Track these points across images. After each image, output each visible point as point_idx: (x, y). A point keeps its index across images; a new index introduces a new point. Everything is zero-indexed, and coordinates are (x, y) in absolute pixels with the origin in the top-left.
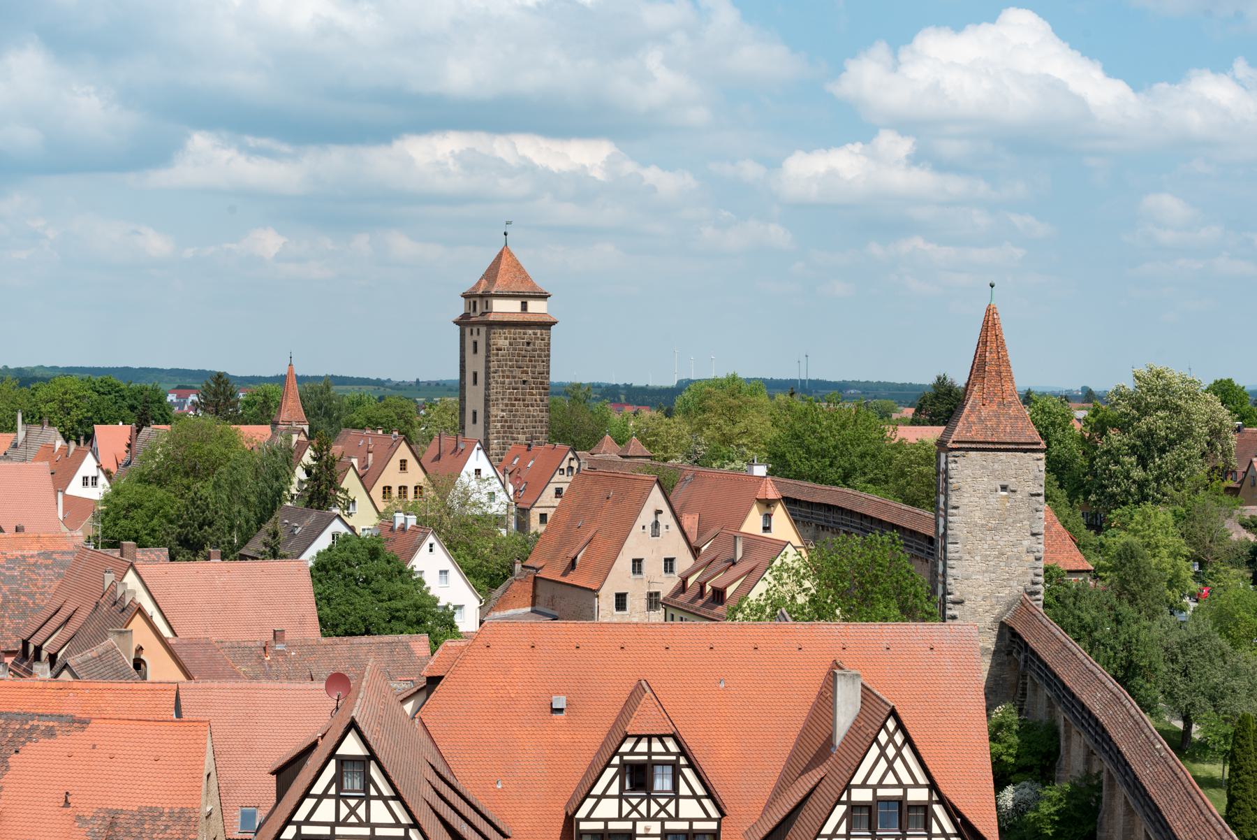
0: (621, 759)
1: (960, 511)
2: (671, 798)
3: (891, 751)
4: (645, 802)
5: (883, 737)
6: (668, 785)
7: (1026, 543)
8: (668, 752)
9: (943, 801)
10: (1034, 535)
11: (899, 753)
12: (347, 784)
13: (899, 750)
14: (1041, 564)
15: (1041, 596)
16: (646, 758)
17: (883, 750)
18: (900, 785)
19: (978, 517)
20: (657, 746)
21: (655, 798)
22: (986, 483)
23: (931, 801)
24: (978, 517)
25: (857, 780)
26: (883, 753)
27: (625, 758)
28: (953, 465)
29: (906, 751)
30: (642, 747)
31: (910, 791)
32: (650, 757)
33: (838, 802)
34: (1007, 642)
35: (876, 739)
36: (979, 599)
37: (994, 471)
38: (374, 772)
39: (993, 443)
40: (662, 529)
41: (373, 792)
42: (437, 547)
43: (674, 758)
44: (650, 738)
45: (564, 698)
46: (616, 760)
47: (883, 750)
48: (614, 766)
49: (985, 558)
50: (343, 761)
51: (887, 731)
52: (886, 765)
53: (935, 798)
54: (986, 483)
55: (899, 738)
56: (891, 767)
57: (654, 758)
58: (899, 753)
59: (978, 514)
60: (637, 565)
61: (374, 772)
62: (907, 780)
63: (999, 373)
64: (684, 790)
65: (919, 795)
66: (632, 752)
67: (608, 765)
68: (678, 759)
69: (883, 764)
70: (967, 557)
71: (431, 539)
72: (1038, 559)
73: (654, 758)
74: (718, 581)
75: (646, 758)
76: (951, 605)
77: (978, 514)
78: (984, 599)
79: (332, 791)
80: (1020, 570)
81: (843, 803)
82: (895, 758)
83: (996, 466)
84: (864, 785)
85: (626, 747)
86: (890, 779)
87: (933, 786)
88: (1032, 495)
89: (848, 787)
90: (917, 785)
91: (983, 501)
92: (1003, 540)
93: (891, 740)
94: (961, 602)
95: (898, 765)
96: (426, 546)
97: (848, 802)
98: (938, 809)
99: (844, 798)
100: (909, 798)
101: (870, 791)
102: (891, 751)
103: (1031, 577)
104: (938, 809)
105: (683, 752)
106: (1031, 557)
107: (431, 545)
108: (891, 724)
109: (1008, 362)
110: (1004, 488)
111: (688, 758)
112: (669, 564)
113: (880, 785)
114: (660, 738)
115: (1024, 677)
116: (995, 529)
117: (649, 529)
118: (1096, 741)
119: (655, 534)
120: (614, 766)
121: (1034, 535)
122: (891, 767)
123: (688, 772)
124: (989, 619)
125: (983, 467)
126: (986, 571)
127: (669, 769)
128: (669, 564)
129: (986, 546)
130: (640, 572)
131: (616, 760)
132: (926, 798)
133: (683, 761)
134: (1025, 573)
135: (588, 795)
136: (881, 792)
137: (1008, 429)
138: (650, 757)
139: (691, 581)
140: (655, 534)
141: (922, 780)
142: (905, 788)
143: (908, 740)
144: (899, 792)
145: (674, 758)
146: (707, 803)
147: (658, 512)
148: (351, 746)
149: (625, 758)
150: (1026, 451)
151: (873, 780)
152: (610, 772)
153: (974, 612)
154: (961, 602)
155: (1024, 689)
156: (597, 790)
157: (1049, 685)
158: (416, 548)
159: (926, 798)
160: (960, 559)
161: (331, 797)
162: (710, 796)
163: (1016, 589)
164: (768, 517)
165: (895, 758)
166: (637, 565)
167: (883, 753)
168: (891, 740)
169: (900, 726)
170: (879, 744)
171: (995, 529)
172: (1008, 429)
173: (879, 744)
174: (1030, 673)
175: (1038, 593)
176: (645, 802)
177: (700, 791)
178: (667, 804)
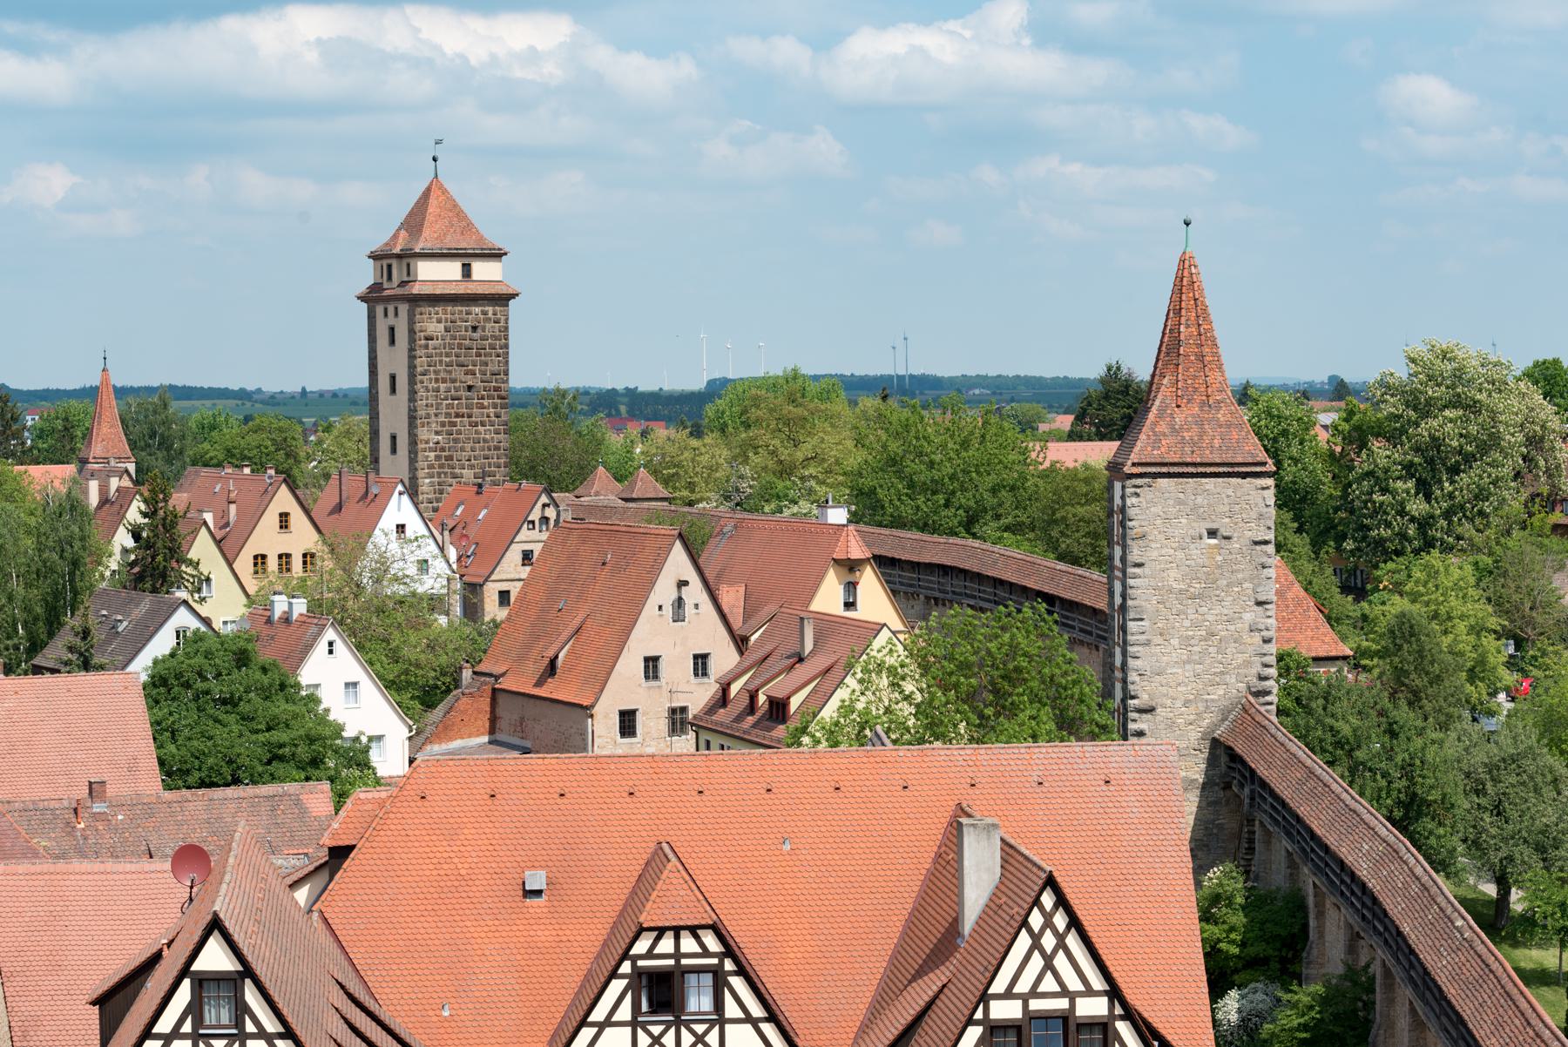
0: (634, 965)
1: (1146, 570)
2: (712, 1023)
3: (1049, 941)
4: (672, 1031)
5: (1036, 920)
6: (706, 1003)
7: (1248, 617)
8: (706, 953)
9: (1130, 1015)
10: (1259, 604)
11: (1061, 944)
12: (210, 1016)
14: (1272, 648)
15: (1273, 698)
16: (671, 962)
17: (1036, 939)
18: (1064, 992)
19: (1173, 578)
20: (688, 944)
21: (687, 1024)
22: (1186, 526)
23: (1112, 1016)
24: (1173, 578)
25: (998, 986)
26: (1036, 944)
27: (640, 963)
28: (1134, 500)
29: (1072, 941)
30: (666, 945)
31: (1079, 1001)
32: (677, 961)
33: (970, 1021)
34: (1223, 768)
35: (1025, 923)
36: (1179, 704)
37: (1196, 508)
38: (251, 997)
39: (1194, 465)
40: (689, 610)
41: (250, 1027)
42: (339, 646)
43: (715, 961)
44: (677, 931)
45: (542, 874)
46: (626, 967)
47: (1036, 939)
48: (623, 976)
49: (1187, 642)
50: (203, 982)
52: (1042, 963)
53: (1118, 1011)
55: (1060, 921)
56: (1049, 965)
57: (684, 961)
58: (1061, 944)
59: (1173, 574)
60: (652, 665)
61: (251, 997)
62: (1074, 984)
63: (1201, 357)
64: (731, 1010)
65: (1094, 1007)
66: (650, 954)
67: (614, 974)
68: (722, 963)
69: (1037, 962)
70: (1158, 640)
71: (330, 634)
72: (1267, 641)
73: (684, 961)
74: (777, 688)
75: (671, 962)
76: (1132, 715)
77: (1173, 574)
78: (1186, 703)
79: (187, 1028)
80: (1240, 659)
81: (977, 1023)
82: (1055, 951)
83: (1199, 500)
84: (1008, 994)
85: (641, 947)
86: (1049, 984)
87: (1114, 993)
88: (1256, 543)
89: (984, 998)
90: (1089, 992)
91: (1180, 555)
92: (1212, 613)
93: (1048, 923)
94: (1150, 710)
95: (1060, 961)
96: (322, 646)
97: (986, 1021)
98: (1123, 1028)
99: (979, 1015)
100: (1078, 1013)
101: (1019, 1002)
102: (1049, 941)
103: (1257, 669)
104: (1123, 1028)
105: (729, 952)
106: (1257, 638)
107: (331, 644)
108: (1048, 900)
109: (1214, 340)
110: (1212, 533)
111: (736, 961)
112: (701, 663)
113: (1034, 993)
114: (694, 930)
115: (1251, 822)
116: (1200, 596)
117: (668, 611)
118: (1364, 917)
119: (678, 616)
120: (623, 976)
121: (1259, 604)
122: (1049, 965)
123: (737, 983)
124: (1194, 735)
125: (1180, 502)
126: (1188, 662)
127: (707, 979)
128: (701, 663)
129: (1187, 623)
130: (656, 677)
131: (626, 967)
132: (1106, 1012)
133: (729, 965)
134: (1247, 664)
135: (583, 1023)
136: (1035, 1005)
137: (1217, 443)
138: (677, 961)
139: (735, 688)
140: (678, 616)
141: (1098, 983)
143: (1074, 923)
144: (1063, 1004)
145: (715, 961)
146: (768, 1029)
147: (682, 584)
148: (215, 958)
149: (640, 963)
150: (1244, 476)
151: (1023, 986)
152: (617, 986)
153: (1171, 725)
154: (1150, 710)
155: (1251, 841)
156: (598, 1014)
157: (1289, 834)
158: (307, 649)
159: (1106, 1012)
160: (1147, 643)
161: (185, 1036)
162: (772, 1018)
163: (1234, 687)
164: (851, 587)
165: (1055, 951)
166: (652, 665)
167: (1036, 944)
168: (1048, 923)
169: (1062, 902)
170: (1030, 931)
171: (1200, 596)
172: (1217, 443)
173: (1030, 931)
174: (1259, 816)
175: (1268, 693)
176: (672, 1031)
177: (757, 1011)
178: (707, 1032)
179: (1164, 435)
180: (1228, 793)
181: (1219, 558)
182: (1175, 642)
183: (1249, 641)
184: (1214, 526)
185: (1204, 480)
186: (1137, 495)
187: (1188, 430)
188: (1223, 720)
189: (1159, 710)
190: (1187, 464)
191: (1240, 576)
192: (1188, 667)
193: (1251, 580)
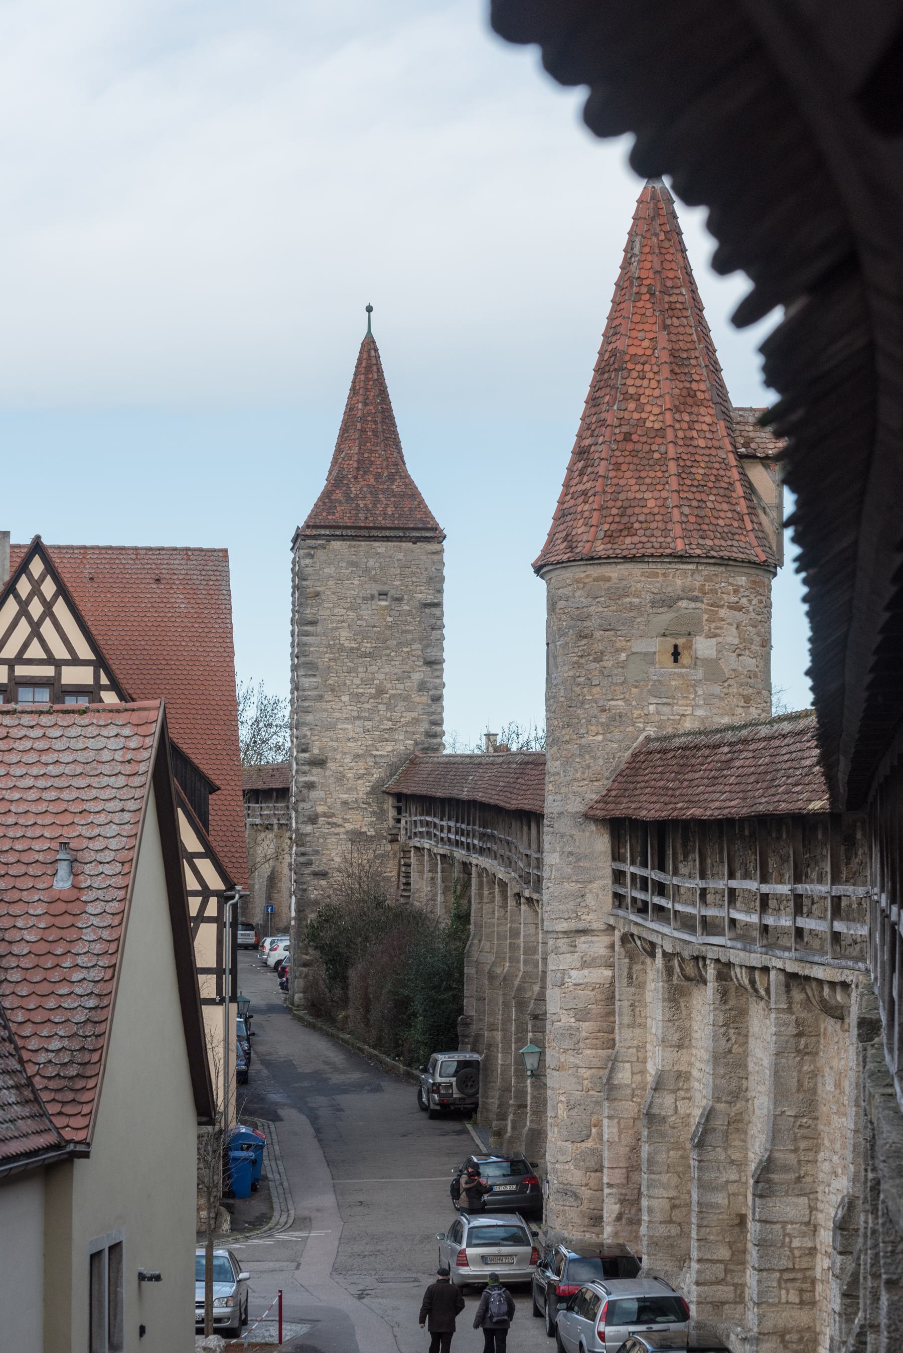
1: (319, 629)
3: (36, 609)
5: (24, 587)
7: (417, 676)
11: (48, 612)
13: (48, 607)
18: (50, 660)
22: (355, 587)
26: (23, 611)
31: (64, 669)
37: (367, 570)
51: (30, 577)
53: (104, 680)
54: (355, 587)
56: (35, 632)
58: (48, 612)
62: (61, 652)
70: (328, 696)
83: (371, 563)
87: (100, 663)
90: (75, 661)
91: (352, 615)
92: (382, 671)
93: (36, 591)
95: (47, 629)
100: (63, 682)
102: (36, 609)
122: (35, 632)
126: (359, 718)
132: (91, 682)
134: (416, 721)
136: (21, 671)
137: (390, 511)
141: (84, 651)
142: (58, 664)
143: (62, 591)
144: (48, 671)
153: (340, 778)
159: (91, 682)
160: (320, 698)
167: (23, 611)
168: (36, 591)
172: (390, 511)
179: (340, 502)
180: (396, 847)
181: (389, 619)
182: (345, 698)
183: (417, 699)
184: (385, 588)
185: (376, 544)
186: (312, 557)
187: (364, 498)
188: (391, 775)
189: (330, 764)
190: (360, 528)
191: (409, 637)
192: (357, 723)
193: (421, 640)
